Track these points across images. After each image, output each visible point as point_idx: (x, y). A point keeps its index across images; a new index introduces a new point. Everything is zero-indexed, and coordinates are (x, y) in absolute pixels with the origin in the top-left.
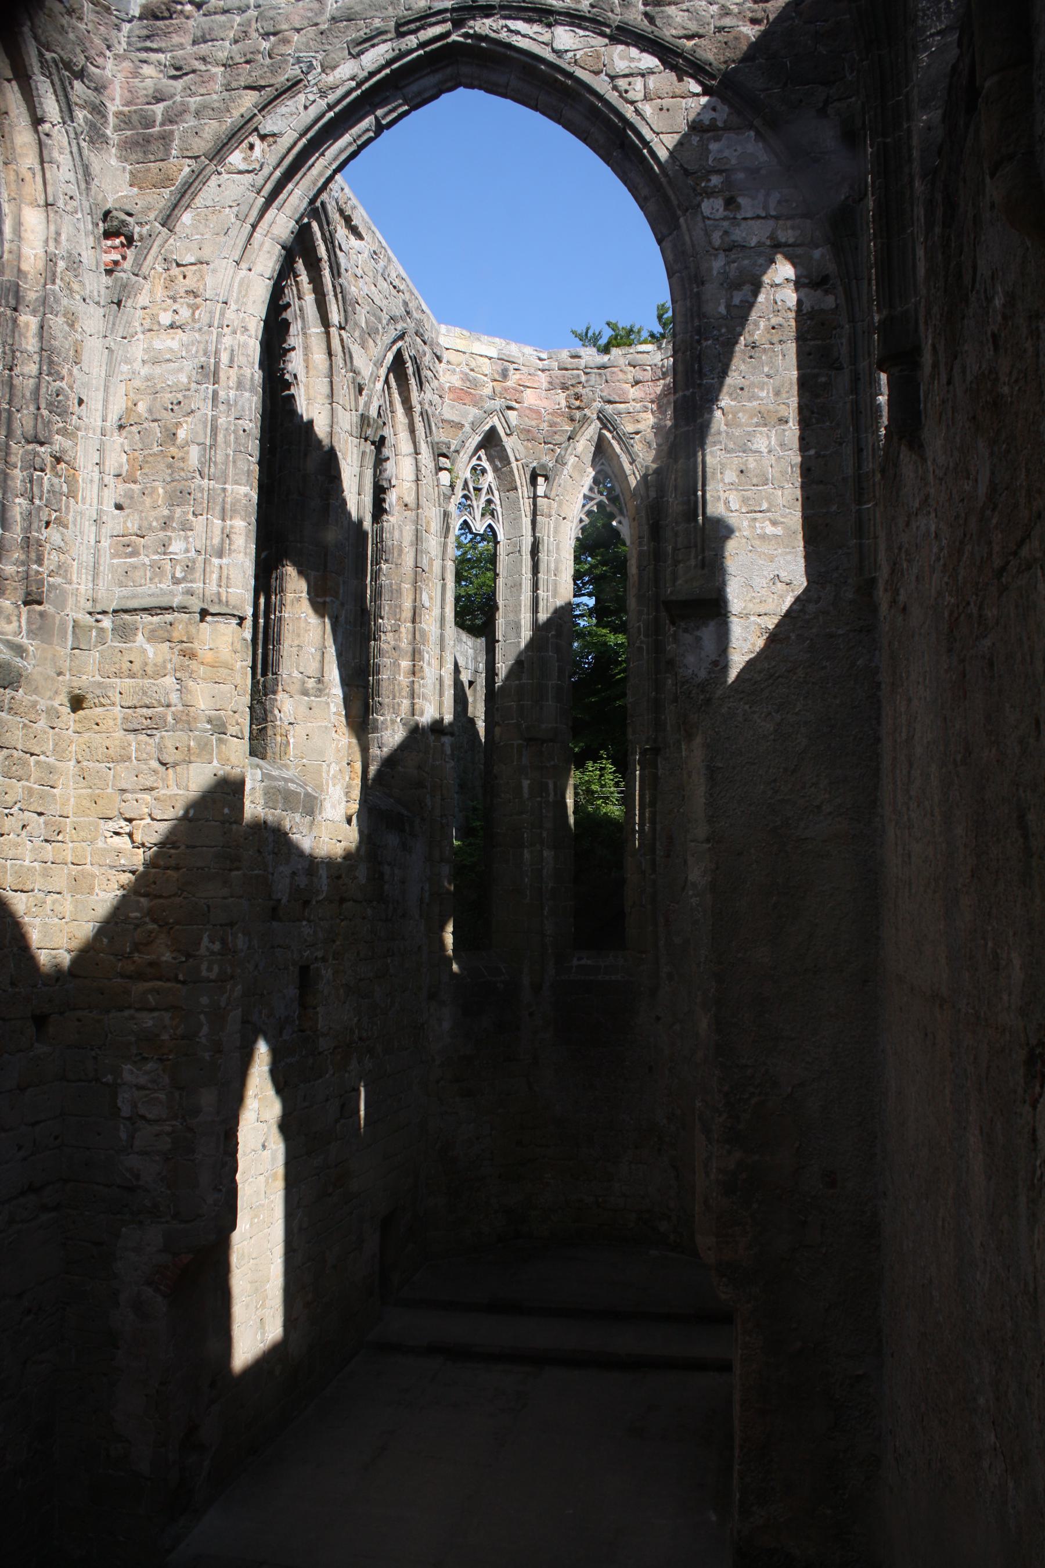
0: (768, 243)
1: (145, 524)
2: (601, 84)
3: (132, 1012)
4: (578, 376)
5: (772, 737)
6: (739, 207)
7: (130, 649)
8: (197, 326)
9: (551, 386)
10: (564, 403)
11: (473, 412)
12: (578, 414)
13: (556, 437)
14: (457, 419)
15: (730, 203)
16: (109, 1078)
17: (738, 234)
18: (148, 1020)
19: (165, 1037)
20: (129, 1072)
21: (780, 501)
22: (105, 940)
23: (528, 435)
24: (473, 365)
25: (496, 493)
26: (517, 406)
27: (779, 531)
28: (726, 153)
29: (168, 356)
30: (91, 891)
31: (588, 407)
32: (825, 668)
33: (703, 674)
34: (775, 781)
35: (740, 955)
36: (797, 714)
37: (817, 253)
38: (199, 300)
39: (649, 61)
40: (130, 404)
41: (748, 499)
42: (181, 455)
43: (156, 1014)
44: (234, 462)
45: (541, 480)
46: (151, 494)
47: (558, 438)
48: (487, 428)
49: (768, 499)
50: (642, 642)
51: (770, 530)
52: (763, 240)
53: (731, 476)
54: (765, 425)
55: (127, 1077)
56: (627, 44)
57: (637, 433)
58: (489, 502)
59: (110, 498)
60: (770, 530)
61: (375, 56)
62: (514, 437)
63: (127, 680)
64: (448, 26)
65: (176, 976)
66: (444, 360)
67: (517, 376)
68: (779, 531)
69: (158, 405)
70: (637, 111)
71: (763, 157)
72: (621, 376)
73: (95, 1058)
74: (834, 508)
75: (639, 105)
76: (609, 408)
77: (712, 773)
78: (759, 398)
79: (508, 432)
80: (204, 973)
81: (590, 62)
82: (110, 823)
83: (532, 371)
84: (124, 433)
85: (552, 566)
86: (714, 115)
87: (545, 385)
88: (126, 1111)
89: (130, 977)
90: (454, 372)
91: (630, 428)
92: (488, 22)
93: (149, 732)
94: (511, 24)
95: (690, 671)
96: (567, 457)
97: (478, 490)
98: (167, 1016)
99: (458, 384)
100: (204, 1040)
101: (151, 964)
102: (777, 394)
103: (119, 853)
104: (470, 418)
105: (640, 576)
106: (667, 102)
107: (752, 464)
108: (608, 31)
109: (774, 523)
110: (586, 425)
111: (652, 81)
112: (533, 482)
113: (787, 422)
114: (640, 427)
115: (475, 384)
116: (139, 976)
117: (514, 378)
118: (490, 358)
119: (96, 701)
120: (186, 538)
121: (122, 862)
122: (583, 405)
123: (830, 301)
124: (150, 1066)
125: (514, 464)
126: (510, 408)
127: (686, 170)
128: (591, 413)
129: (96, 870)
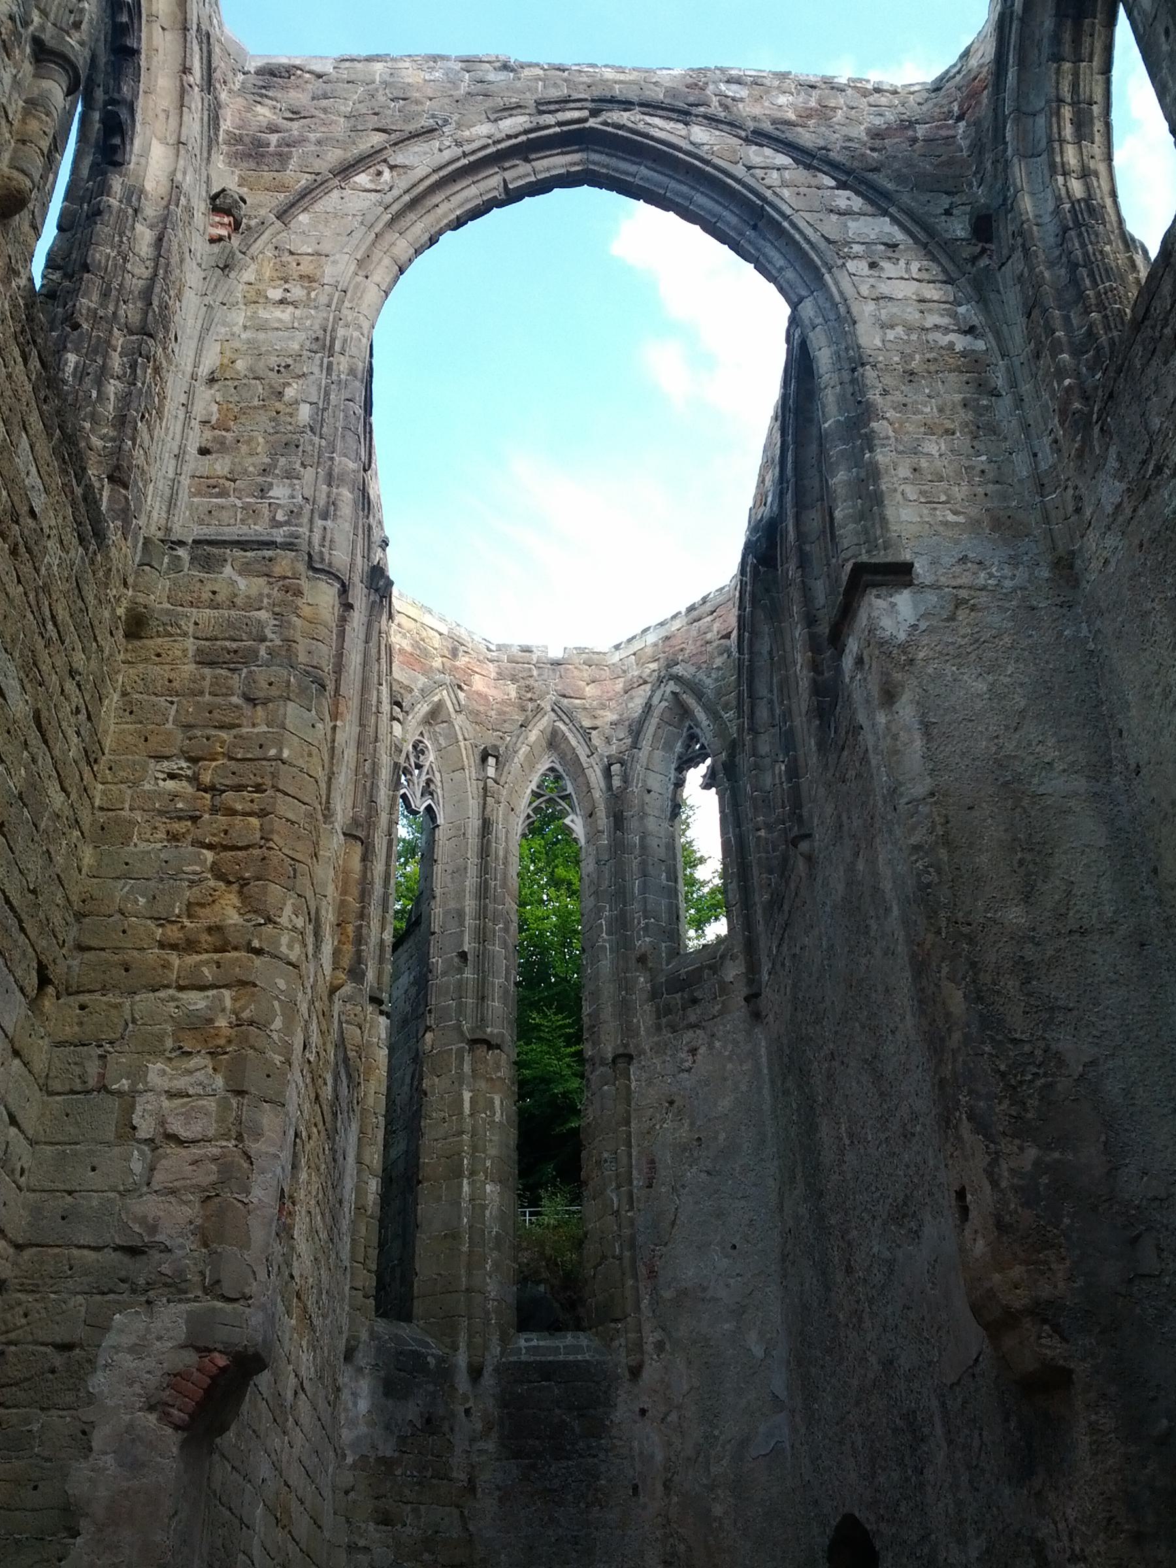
0: (914, 297)
1: (239, 468)
2: (739, 171)
3: (171, 992)
4: (530, 669)
5: (987, 696)
6: (882, 269)
7: (216, 580)
8: (312, 304)
9: (500, 676)
10: (513, 694)
11: (422, 681)
12: (530, 705)
13: (506, 725)
14: (406, 682)
15: (873, 265)
16: (125, 1084)
17: (884, 288)
18: (197, 1001)
19: (222, 1022)
20: (158, 1073)
21: (959, 497)
22: (142, 901)
23: (476, 718)
24: (424, 634)
25: (437, 774)
26: (465, 687)
27: (961, 519)
28: (865, 230)
29: (276, 325)
30: (126, 840)
31: (541, 698)
32: (1031, 636)
33: (902, 636)
34: (997, 737)
35: (989, 915)
36: (1010, 676)
37: (962, 310)
38: (314, 285)
39: (782, 160)
40: (226, 361)
41: (926, 492)
42: (287, 410)
43: (210, 993)
44: (343, 437)
45: (491, 761)
46: (248, 442)
47: (507, 726)
48: (436, 699)
49: (945, 493)
50: (604, 941)
51: (951, 518)
52: (909, 295)
53: (904, 472)
54: (934, 434)
55: (154, 1078)
56: (761, 145)
57: (594, 728)
58: (429, 782)
59: (196, 438)
60: (951, 518)
61: (509, 125)
62: (461, 717)
63: (207, 610)
64: (586, 113)
65: (249, 943)
66: (396, 622)
67: (467, 659)
68: (961, 519)
69: (261, 364)
70: (775, 193)
71: (899, 236)
72: (576, 673)
73: (102, 1057)
74: (1014, 503)
75: (778, 190)
76: (566, 701)
77: (927, 728)
78: (922, 413)
79: (457, 708)
80: (284, 949)
81: (727, 155)
82: (166, 764)
83: (481, 658)
84: (216, 386)
85: (501, 854)
86: (848, 202)
87: (493, 675)
88: (146, 1127)
89: (174, 947)
90: (404, 636)
91: (587, 723)
92: (626, 115)
93: (232, 666)
94: (647, 118)
95: (888, 633)
96: (519, 745)
97: (419, 767)
98: (227, 994)
99: (409, 649)
100: (275, 1036)
101: (210, 930)
102: (941, 410)
103: (174, 796)
104: (420, 685)
105: (600, 873)
106: (802, 190)
107: (924, 464)
108: (743, 134)
109: (955, 513)
110: (539, 716)
111: (787, 174)
112: (484, 759)
113: (953, 434)
114: (598, 723)
115: (426, 653)
116: (190, 946)
117: (462, 661)
118: (441, 634)
119: (161, 629)
120: (292, 486)
121: (180, 805)
122: (535, 697)
123: (980, 345)
124: (193, 1063)
125: (462, 744)
126: (460, 687)
127: (827, 239)
128: (546, 705)
129: (138, 816)
